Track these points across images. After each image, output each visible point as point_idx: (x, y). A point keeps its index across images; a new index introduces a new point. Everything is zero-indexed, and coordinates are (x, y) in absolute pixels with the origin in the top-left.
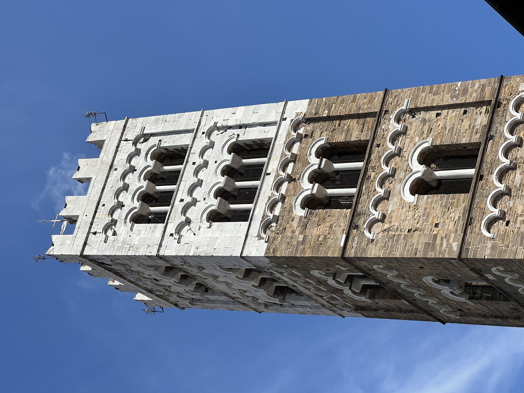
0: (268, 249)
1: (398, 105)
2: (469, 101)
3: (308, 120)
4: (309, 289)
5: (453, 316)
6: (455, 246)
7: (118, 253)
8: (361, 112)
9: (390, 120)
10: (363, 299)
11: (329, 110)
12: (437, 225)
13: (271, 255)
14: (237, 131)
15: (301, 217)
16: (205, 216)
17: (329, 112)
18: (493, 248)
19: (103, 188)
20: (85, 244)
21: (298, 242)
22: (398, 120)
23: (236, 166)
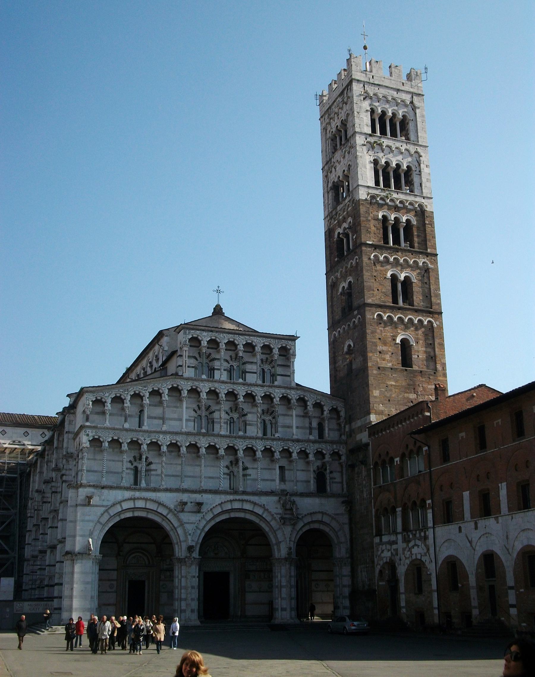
0: (363, 200)
1: (431, 262)
2: (432, 299)
6: (369, 301)
8: (428, 242)
9: (424, 259)
10: (336, 236)
11: (428, 224)
12: (378, 290)
13: (361, 203)
15: (378, 216)
17: (428, 224)
18: (370, 318)
19: (387, 87)
20: (358, 81)
22: (424, 263)
23: (400, 170)
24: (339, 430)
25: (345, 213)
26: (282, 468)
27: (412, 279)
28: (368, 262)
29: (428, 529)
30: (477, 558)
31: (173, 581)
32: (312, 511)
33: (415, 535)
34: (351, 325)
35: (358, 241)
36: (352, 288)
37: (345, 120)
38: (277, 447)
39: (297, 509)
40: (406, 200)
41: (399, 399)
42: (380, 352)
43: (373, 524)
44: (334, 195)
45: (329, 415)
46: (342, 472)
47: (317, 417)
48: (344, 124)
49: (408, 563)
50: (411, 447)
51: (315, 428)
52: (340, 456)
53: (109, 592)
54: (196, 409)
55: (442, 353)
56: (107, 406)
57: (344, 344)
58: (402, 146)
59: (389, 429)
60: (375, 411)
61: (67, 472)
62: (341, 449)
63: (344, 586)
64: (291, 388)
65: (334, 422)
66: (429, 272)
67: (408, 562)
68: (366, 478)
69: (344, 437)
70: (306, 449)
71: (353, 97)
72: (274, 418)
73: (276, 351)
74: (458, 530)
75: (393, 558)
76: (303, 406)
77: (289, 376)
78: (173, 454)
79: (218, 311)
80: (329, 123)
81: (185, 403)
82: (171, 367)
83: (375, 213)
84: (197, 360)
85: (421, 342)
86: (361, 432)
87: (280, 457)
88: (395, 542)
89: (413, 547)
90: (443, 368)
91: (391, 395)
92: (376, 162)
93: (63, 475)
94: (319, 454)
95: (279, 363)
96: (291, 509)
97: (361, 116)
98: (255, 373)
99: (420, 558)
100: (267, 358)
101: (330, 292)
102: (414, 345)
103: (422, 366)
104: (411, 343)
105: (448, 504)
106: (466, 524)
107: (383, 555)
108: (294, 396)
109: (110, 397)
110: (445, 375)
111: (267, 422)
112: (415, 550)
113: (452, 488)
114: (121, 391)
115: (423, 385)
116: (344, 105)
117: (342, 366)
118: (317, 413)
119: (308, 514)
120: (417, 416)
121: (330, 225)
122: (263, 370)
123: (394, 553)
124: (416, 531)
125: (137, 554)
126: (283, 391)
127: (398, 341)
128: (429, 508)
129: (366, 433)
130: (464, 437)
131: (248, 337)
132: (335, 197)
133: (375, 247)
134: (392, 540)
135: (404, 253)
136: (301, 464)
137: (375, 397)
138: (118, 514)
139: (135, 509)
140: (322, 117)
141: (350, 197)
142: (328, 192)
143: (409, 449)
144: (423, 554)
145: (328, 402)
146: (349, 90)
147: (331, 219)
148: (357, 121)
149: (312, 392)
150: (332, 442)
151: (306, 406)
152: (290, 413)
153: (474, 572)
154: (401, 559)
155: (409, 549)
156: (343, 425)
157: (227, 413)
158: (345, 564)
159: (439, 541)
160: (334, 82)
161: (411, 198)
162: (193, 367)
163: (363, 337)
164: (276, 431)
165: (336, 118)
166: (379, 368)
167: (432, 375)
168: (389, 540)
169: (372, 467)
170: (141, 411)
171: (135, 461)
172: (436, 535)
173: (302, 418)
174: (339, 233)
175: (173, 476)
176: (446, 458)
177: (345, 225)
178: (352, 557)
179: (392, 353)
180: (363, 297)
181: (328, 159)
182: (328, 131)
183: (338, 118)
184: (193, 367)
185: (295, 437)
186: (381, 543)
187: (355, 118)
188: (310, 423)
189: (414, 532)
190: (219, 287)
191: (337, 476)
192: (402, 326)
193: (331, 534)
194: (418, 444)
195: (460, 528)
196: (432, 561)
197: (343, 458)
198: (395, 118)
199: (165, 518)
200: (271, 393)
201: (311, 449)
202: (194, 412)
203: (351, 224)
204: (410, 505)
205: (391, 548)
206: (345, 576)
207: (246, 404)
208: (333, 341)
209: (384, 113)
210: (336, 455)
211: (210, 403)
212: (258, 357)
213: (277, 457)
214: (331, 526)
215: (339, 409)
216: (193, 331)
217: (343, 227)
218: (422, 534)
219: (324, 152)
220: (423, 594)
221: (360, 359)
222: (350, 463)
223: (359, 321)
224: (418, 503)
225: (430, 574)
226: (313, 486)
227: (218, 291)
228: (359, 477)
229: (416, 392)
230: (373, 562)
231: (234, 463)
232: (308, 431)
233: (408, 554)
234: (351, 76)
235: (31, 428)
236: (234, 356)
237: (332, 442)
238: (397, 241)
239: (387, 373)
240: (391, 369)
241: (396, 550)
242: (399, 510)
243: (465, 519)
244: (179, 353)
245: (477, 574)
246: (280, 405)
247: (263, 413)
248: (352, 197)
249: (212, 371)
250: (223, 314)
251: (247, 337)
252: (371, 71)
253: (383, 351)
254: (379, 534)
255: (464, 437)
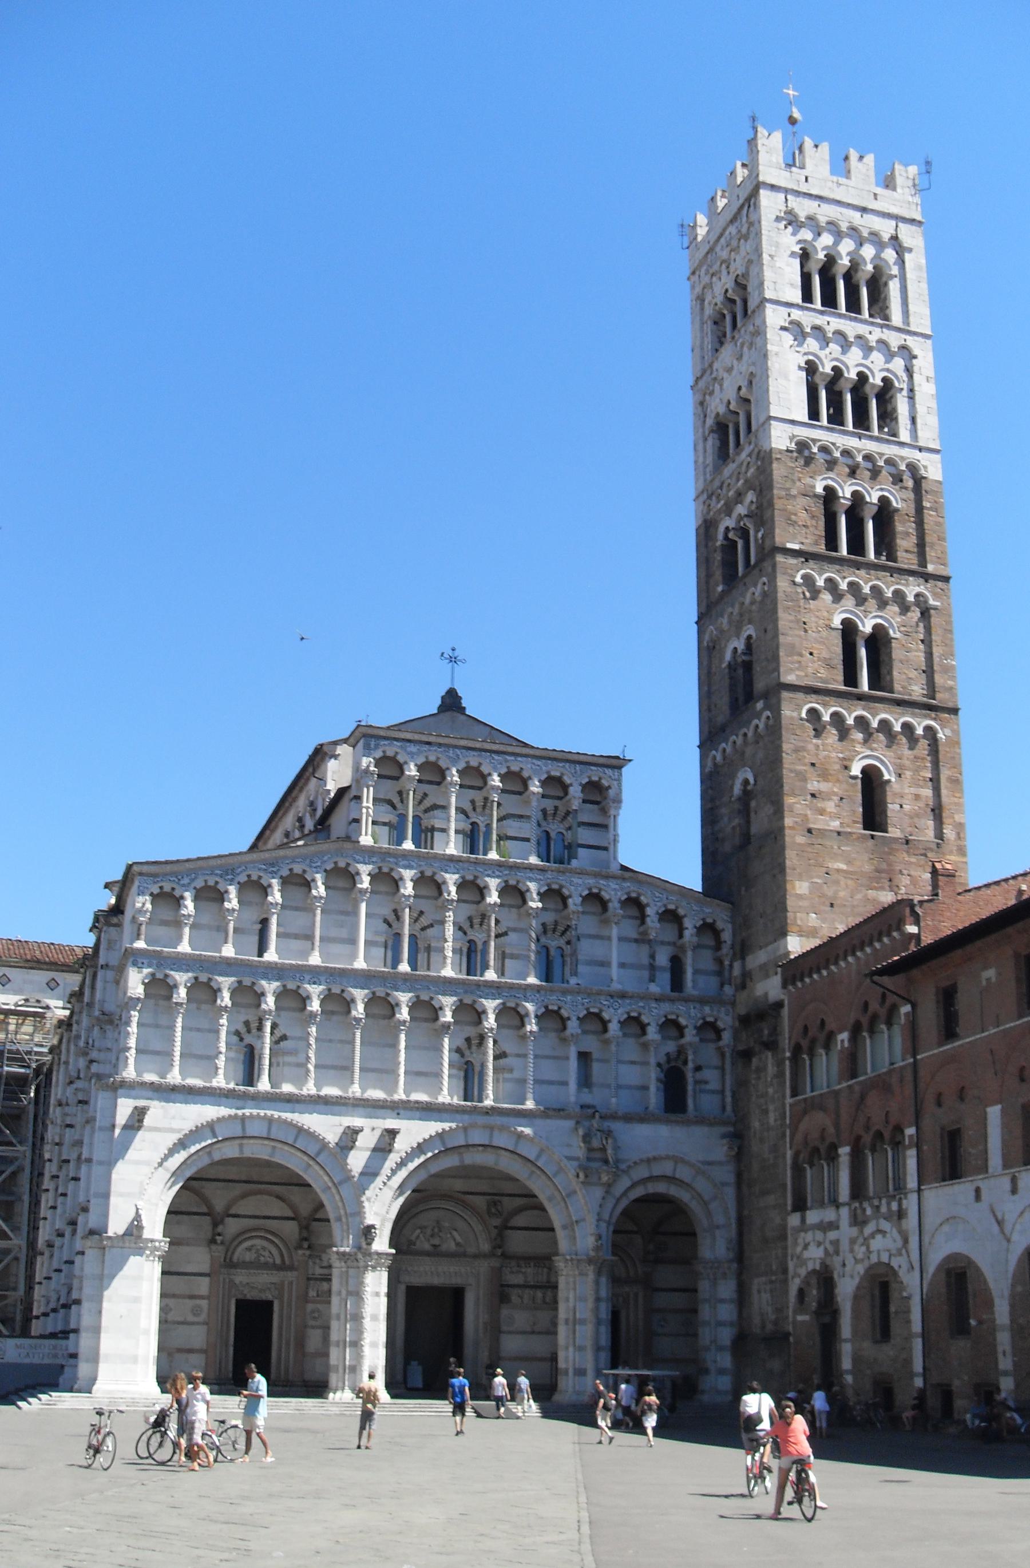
0: (780, 451)
3: (918, 481)
4: (730, 477)
5: (707, 637)
6: (790, 678)
7: (764, 238)
8: (927, 549)
10: (720, 536)
13: (774, 456)
14: (905, 386)
15: (814, 487)
16: (811, 357)
17: (927, 509)
18: (792, 718)
20: (773, 187)
21: (788, 489)
22: (917, 595)
23: (867, 389)
24: (719, 973)
25: (741, 482)
26: (584, 1057)
27: (891, 632)
28: (789, 590)
29: (906, 1194)
30: (1014, 1258)
31: (329, 1302)
32: (650, 1155)
33: (878, 1207)
34: (750, 734)
35: (768, 543)
36: (754, 651)
37: (743, 276)
38: (573, 1009)
39: (617, 1148)
40: (878, 453)
41: (855, 903)
42: (813, 795)
43: (785, 1185)
44: (718, 443)
45: (695, 939)
46: (722, 1069)
47: (669, 943)
48: (741, 285)
49: (862, 1272)
50: (874, 1006)
51: (662, 969)
52: (718, 1032)
53: (193, 1324)
54: (392, 918)
55: (956, 800)
56: (186, 907)
57: (733, 776)
58: (870, 333)
59: (827, 968)
60: (798, 928)
61: (102, 1056)
62: (722, 1015)
63: (720, 1324)
64: (607, 877)
65: (707, 955)
66: (930, 617)
67: (861, 1269)
68: (775, 1081)
69: (728, 990)
70: (640, 1014)
71: (759, 222)
72: (568, 943)
73: (575, 791)
74: (972, 1194)
75: (828, 1262)
76: (636, 918)
77: (606, 849)
78: (335, 1018)
79: (451, 702)
80: (710, 286)
81: (363, 906)
82: (338, 823)
83: (808, 480)
84: (394, 807)
85: (908, 774)
86: (767, 976)
87: (579, 1031)
88: (833, 1226)
89: (872, 1236)
90: (958, 834)
91: (836, 892)
92: (811, 368)
93: (92, 1061)
94: (671, 1026)
95: (584, 818)
96: (603, 1149)
97: (778, 264)
98: (527, 840)
99: (887, 1261)
100: (556, 808)
101: (705, 663)
102: (893, 780)
103: (909, 829)
104: (886, 777)
105: (953, 1138)
106: (992, 1181)
107: (806, 1255)
108: (616, 894)
109: (193, 885)
110: (962, 851)
111: (552, 952)
112: (877, 1243)
113: (962, 1099)
114: (217, 875)
115: (912, 873)
116: (742, 241)
117: (728, 830)
118: (669, 933)
119: (642, 1161)
120: (889, 935)
121: (709, 511)
122: (547, 833)
123: (831, 1249)
124: (880, 1199)
125: (258, 1242)
126: (591, 881)
127: (856, 770)
128: (910, 1147)
129: (776, 980)
130: (994, 980)
131: (513, 758)
132: (720, 448)
133: (806, 556)
134: (827, 1220)
135: (872, 572)
136: (630, 1049)
137: (800, 897)
138: (208, 1150)
139: (245, 1141)
140: (693, 273)
141: (752, 447)
142: (705, 439)
143: (870, 1013)
144: (894, 1252)
145: (695, 908)
146: (752, 208)
147: (710, 497)
148: (768, 274)
149: (658, 887)
150: (702, 1001)
151: (642, 918)
152: (605, 932)
153: (1007, 1293)
154: (847, 1263)
155: (865, 1239)
156: (727, 963)
157: (460, 929)
158: (725, 1274)
159: (929, 1222)
160: (719, 193)
161: (890, 450)
162: (385, 824)
163: (773, 762)
164: (575, 973)
165: (724, 272)
166: (810, 831)
167: (931, 850)
168: (822, 1221)
169: (788, 1054)
170: (265, 922)
171: (249, 1031)
172: (924, 1209)
173: (634, 945)
174: (727, 528)
175: (334, 1067)
176: (949, 1032)
177: (741, 510)
178: (740, 1256)
179: (841, 799)
180: (777, 669)
181: (706, 365)
182: (706, 302)
183: (728, 273)
184: (385, 824)
185: (616, 986)
186: (804, 1227)
187: (765, 268)
188: (652, 957)
189: (876, 1202)
190: (453, 650)
191: (711, 1076)
192: (861, 735)
193: (694, 1206)
194: (891, 999)
195: (978, 1191)
196: (913, 1268)
197: (727, 1037)
198: (856, 271)
199: (311, 1162)
200: (561, 887)
201: (652, 1016)
202: (385, 926)
203: (754, 507)
204: (867, 1139)
205: (825, 1239)
206: (722, 1301)
207: (506, 909)
208: (711, 774)
209: (831, 260)
210: (709, 1029)
211: (425, 905)
212: (534, 804)
213: (574, 1031)
214: (693, 1189)
215: (720, 925)
216: (386, 742)
217: (735, 515)
218: (894, 1206)
219: (697, 350)
220: (892, 1341)
221: (769, 809)
222: (741, 1047)
223: (767, 726)
224: (887, 1135)
225: (909, 1298)
226: (654, 1098)
227: (453, 660)
228: (759, 1078)
229: (893, 887)
230: (785, 1271)
231: (475, 1042)
232: (646, 974)
233: (860, 1251)
234: (758, 175)
235: (63, 971)
236: (479, 803)
237: (702, 1001)
238: (857, 545)
239: (828, 843)
240: (839, 833)
241: (836, 1243)
242: (844, 1151)
243: (990, 1170)
244: (353, 792)
245: (1013, 1296)
246: (583, 913)
247: (545, 932)
248: (756, 445)
249: (429, 834)
250: (462, 710)
251: (508, 758)
252: (802, 167)
253: (820, 792)
254: (800, 1206)
255: (994, 980)
